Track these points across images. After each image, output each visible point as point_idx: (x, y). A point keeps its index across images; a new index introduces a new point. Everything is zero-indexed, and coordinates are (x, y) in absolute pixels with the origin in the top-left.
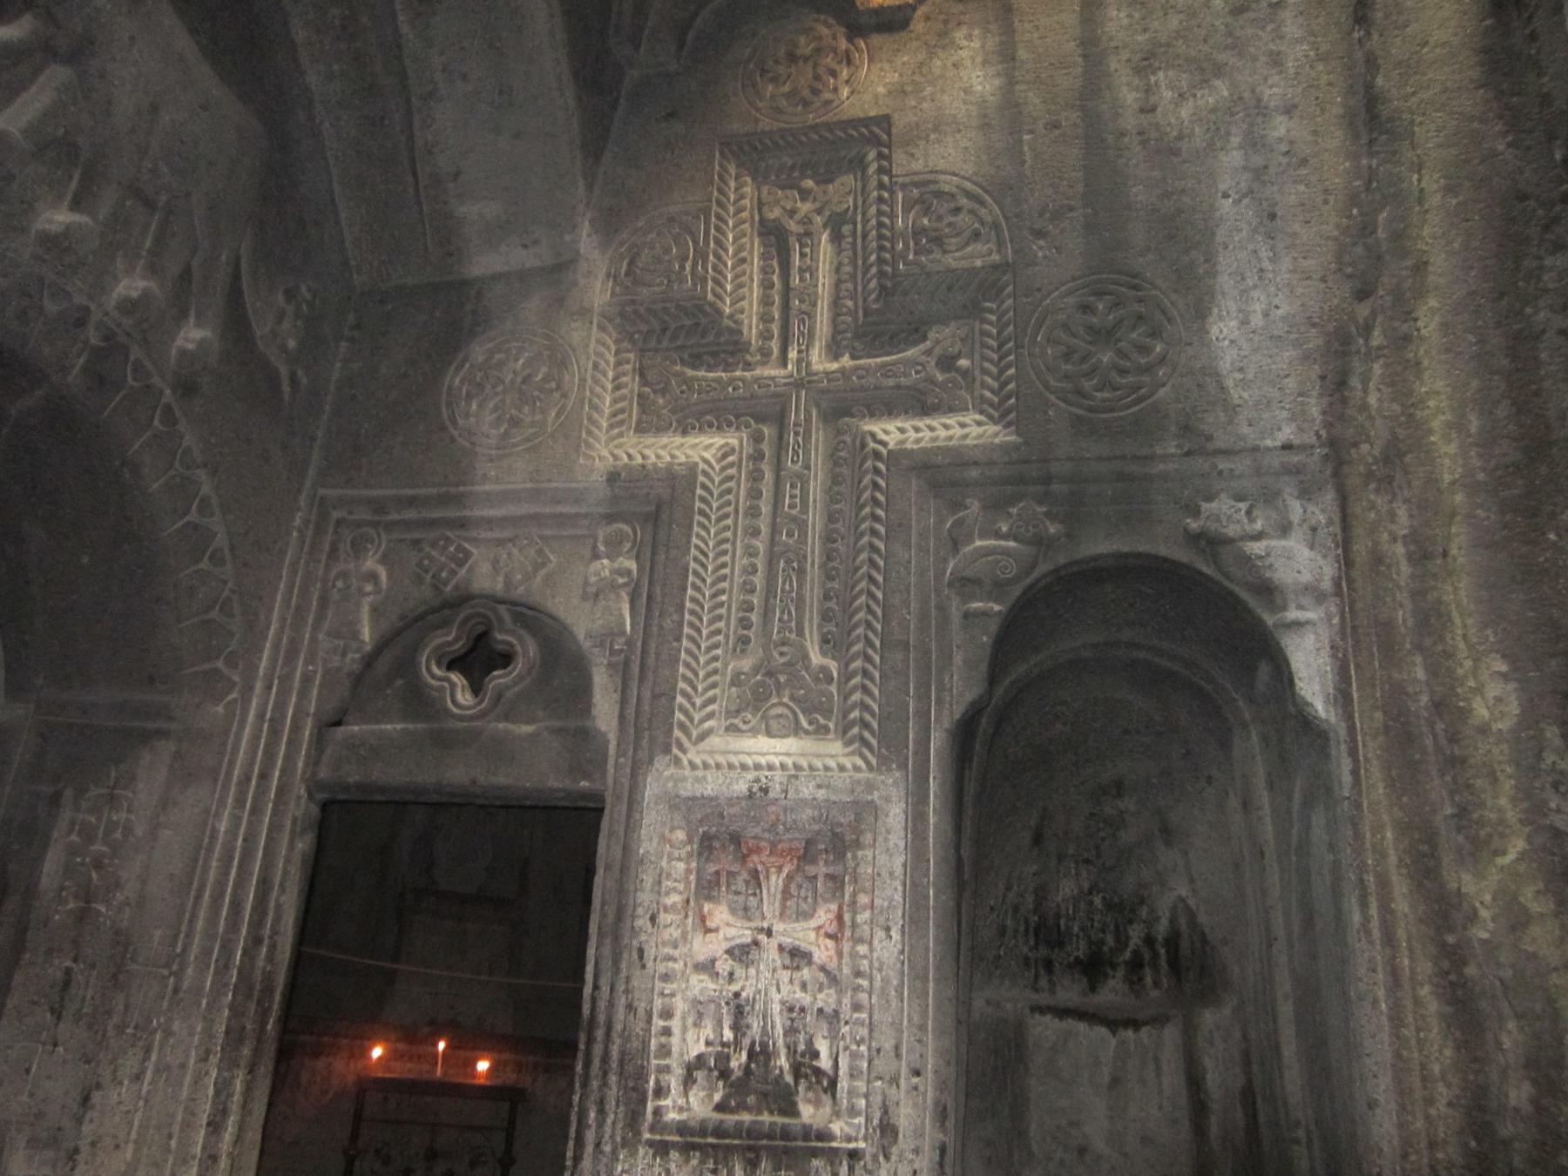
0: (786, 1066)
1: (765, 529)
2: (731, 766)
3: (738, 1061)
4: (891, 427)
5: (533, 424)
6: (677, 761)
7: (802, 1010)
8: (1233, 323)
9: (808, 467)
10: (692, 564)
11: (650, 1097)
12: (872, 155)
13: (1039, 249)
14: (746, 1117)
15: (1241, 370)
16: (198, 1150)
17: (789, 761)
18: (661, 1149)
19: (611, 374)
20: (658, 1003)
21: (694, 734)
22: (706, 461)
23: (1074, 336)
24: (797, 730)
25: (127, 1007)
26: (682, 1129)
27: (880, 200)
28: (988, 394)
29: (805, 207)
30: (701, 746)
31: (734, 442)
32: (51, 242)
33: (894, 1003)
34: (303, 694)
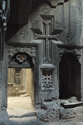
1: (45, 48)
4: (54, 41)
12: (52, 19)
24: (48, 63)
27: (53, 23)
29: (47, 22)
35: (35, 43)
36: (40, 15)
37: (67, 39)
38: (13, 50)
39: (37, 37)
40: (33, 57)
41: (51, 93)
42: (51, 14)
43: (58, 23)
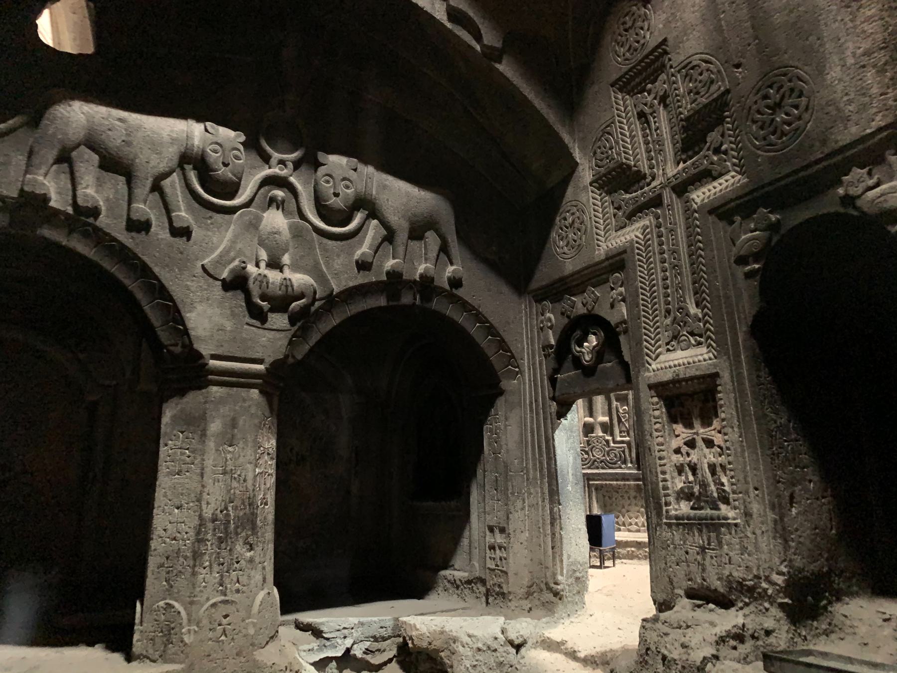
2: (666, 368)
3: (696, 489)
7: (714, 465)
8: (839, 68)
9: (676, 224)
13: (739, 73)
15: (847, 94)
16: (549, 532)
18: (669, 525)
20: (659, 469)
21: (654, 356)
23: (763, 115)
26: (677, 518)
28: (735, 160)
29: (649, 99)
30: (658, 360)
31: (647, 223)
33: (741, 459)
34: (541, 369)
35: (615, 252)
36: (612, 86)
37: (765, 139)
39: (627, 212)
40: (617, 325)
41: (720, 544)
42: (652, 44)
43: (692, 68)
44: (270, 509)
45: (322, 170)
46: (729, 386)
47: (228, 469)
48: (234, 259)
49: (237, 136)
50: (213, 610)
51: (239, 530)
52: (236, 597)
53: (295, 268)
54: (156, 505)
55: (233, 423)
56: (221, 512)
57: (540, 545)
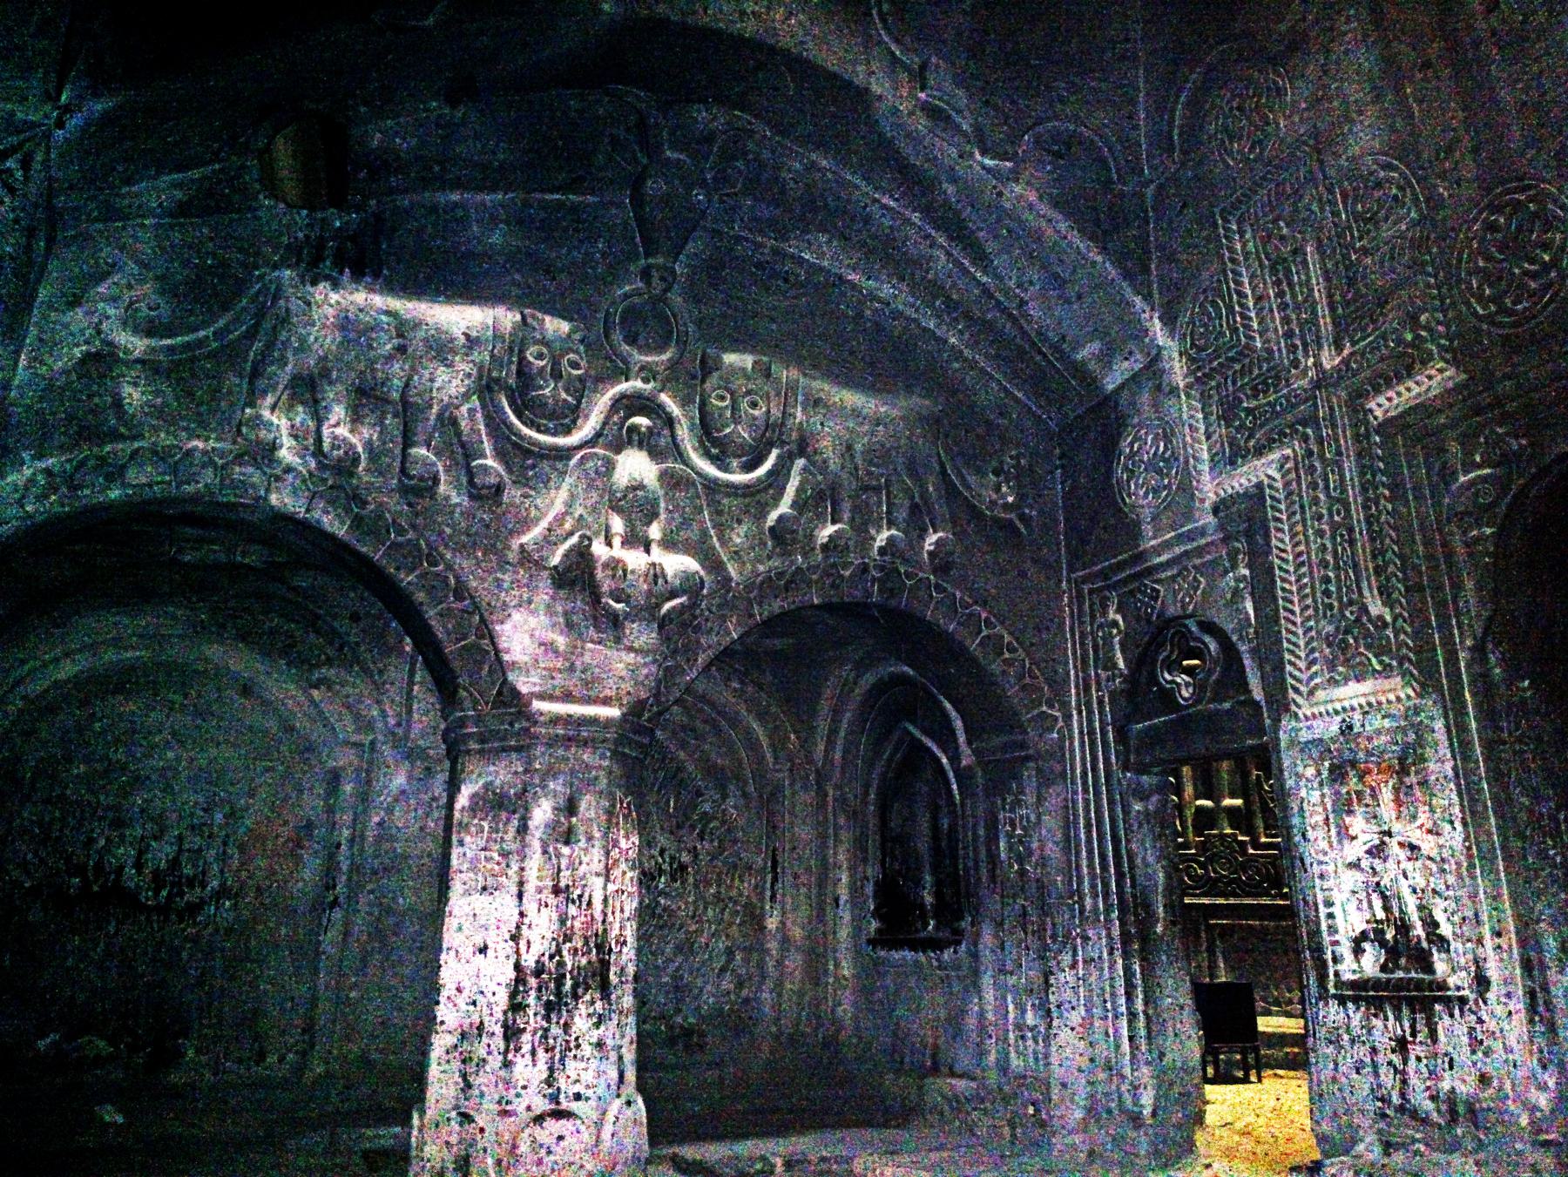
0: (1423, 935)
3: (1389, 936)
5: (1165, 487)
6: (1296, 715)
9: (1339, 453)
10: (1276, 561)
11: (1330, 963)
14: (1400, 974)
16: (1123, 1009)
17: (1363, 701)
18: (1342, 1001)
19: (1202, 428)
20: (1320, 897)
22: (1269, 477)
25: (1054, 925)
26: (1353, 985)
31: (1288, 451)
32: (830, 546)
38: (1119, 618)
44: (629, 952)
45: (713, 380)
46: (1445, 751)
47: (562, 884)
48: (571, 534)
49: (572, 331)
50: (537, 1131)
51: (580, 991)
52: (575, 1106)
53: (669, 544)
54: (445, 946)
55: (571, 808)
56: (551, 957)
57: (1107, 1034)
